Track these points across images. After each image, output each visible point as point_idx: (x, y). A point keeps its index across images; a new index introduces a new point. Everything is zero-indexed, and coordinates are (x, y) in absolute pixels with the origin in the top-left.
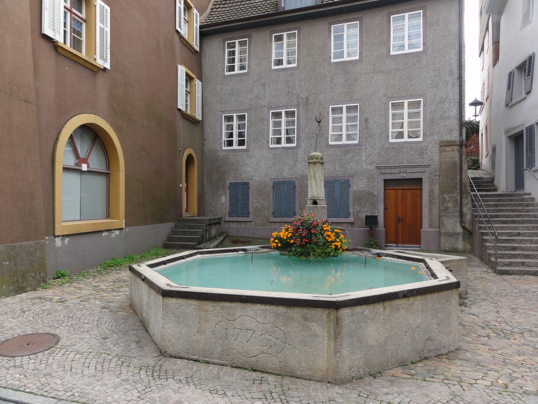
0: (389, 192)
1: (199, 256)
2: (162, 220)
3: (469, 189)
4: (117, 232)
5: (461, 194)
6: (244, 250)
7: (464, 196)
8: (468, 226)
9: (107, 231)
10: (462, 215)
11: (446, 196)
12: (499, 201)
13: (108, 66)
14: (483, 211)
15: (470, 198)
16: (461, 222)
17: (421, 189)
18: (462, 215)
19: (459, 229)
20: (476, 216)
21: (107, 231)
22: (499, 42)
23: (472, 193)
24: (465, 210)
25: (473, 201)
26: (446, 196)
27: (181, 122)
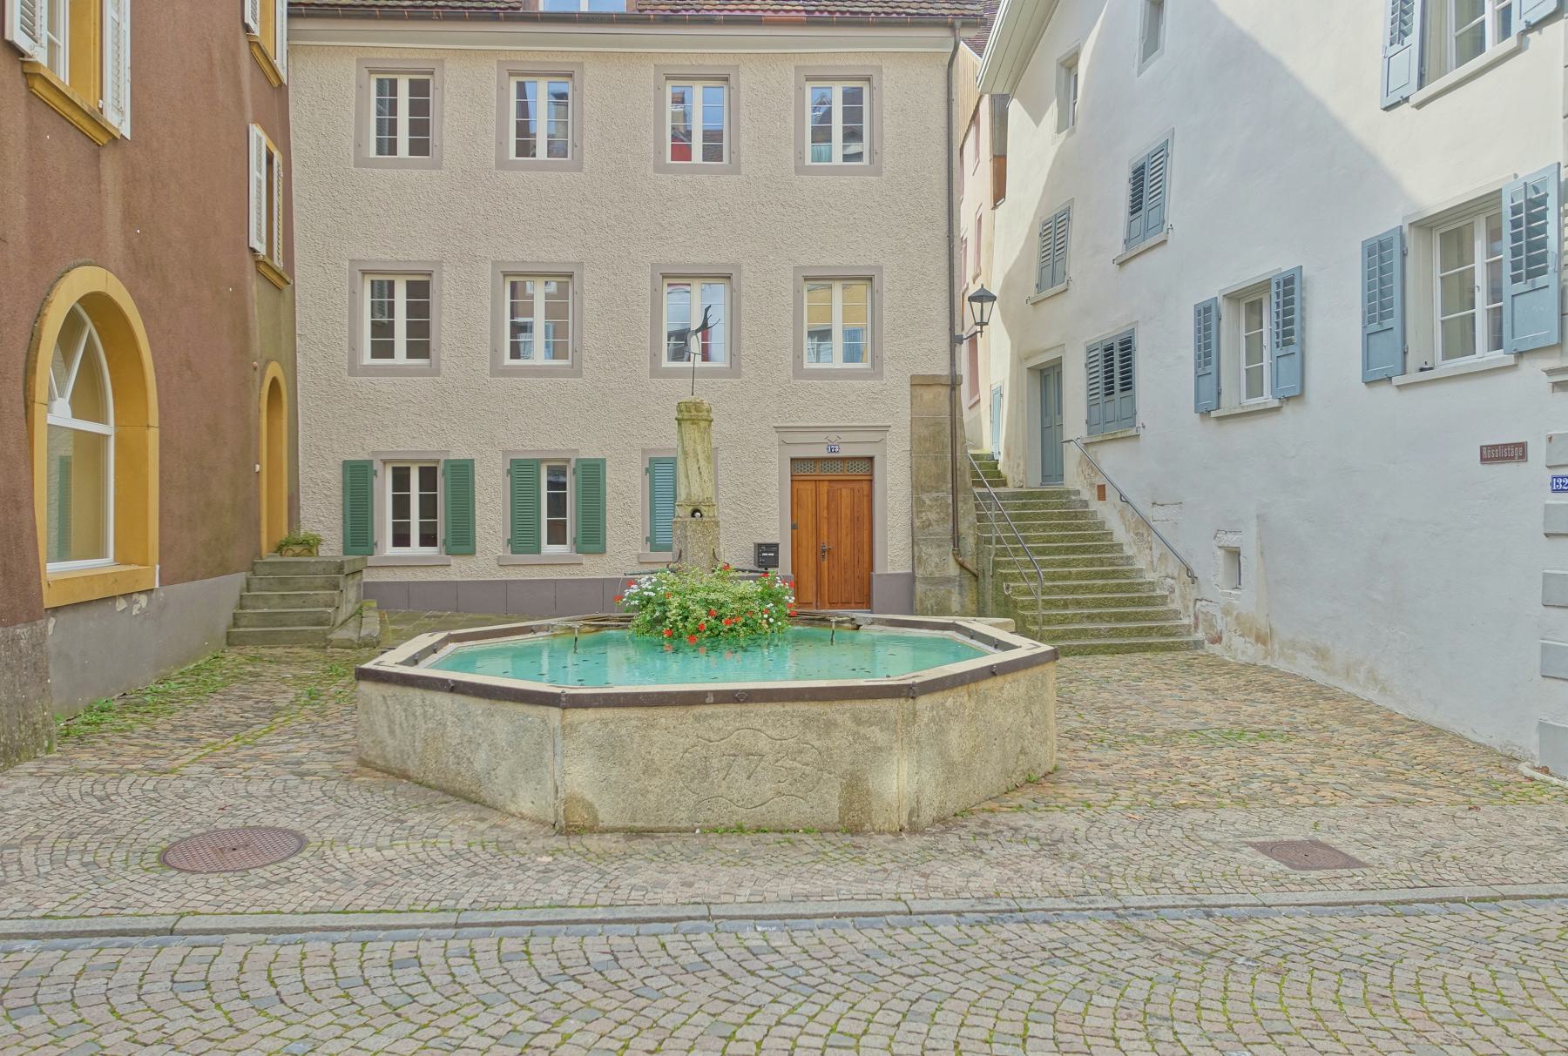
0: (801, 486)
1: (452, 646)
2: (224, 569)
3: (969, 480)
4: (143, 600)
5: (954, 492)
6: (548, 628)
7: (960, 496)
8: (970, 562)
9: (124, 596)
10: (956, 539)
11: (926, 497)
12: (1024, 506)
13: (126, 131)
14: (1008, 529)
15: (972, 502)
16: (957, 553)
17: (871, 481)
18: (956, 539)
19: (953, 570)
20: (989, 541)
21: (124, 596)
22: (1005, 157)
23: (977, 490)
24: (964, 527)
25: (977, 507)
26: (926, 497)
27: (254, 288)
